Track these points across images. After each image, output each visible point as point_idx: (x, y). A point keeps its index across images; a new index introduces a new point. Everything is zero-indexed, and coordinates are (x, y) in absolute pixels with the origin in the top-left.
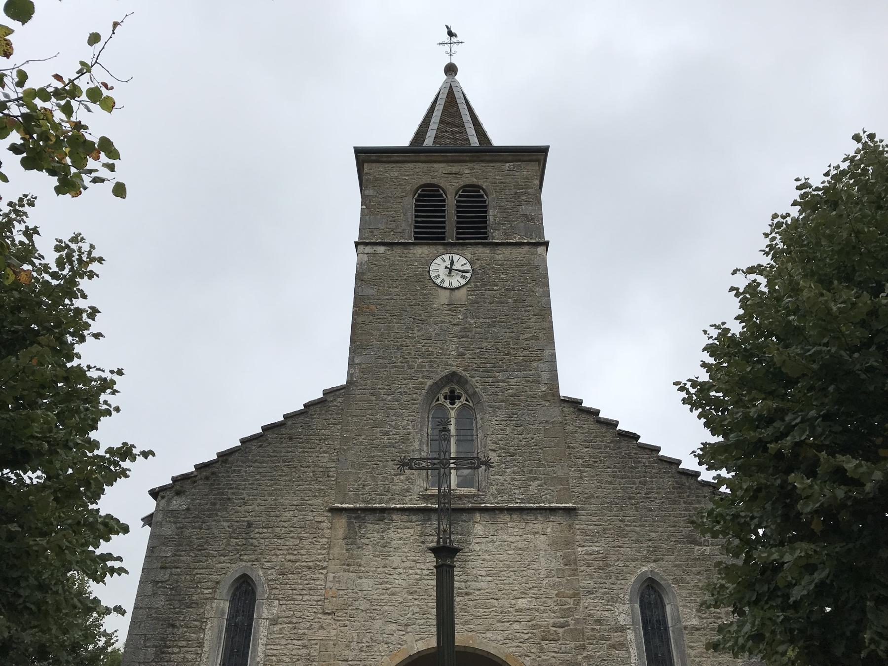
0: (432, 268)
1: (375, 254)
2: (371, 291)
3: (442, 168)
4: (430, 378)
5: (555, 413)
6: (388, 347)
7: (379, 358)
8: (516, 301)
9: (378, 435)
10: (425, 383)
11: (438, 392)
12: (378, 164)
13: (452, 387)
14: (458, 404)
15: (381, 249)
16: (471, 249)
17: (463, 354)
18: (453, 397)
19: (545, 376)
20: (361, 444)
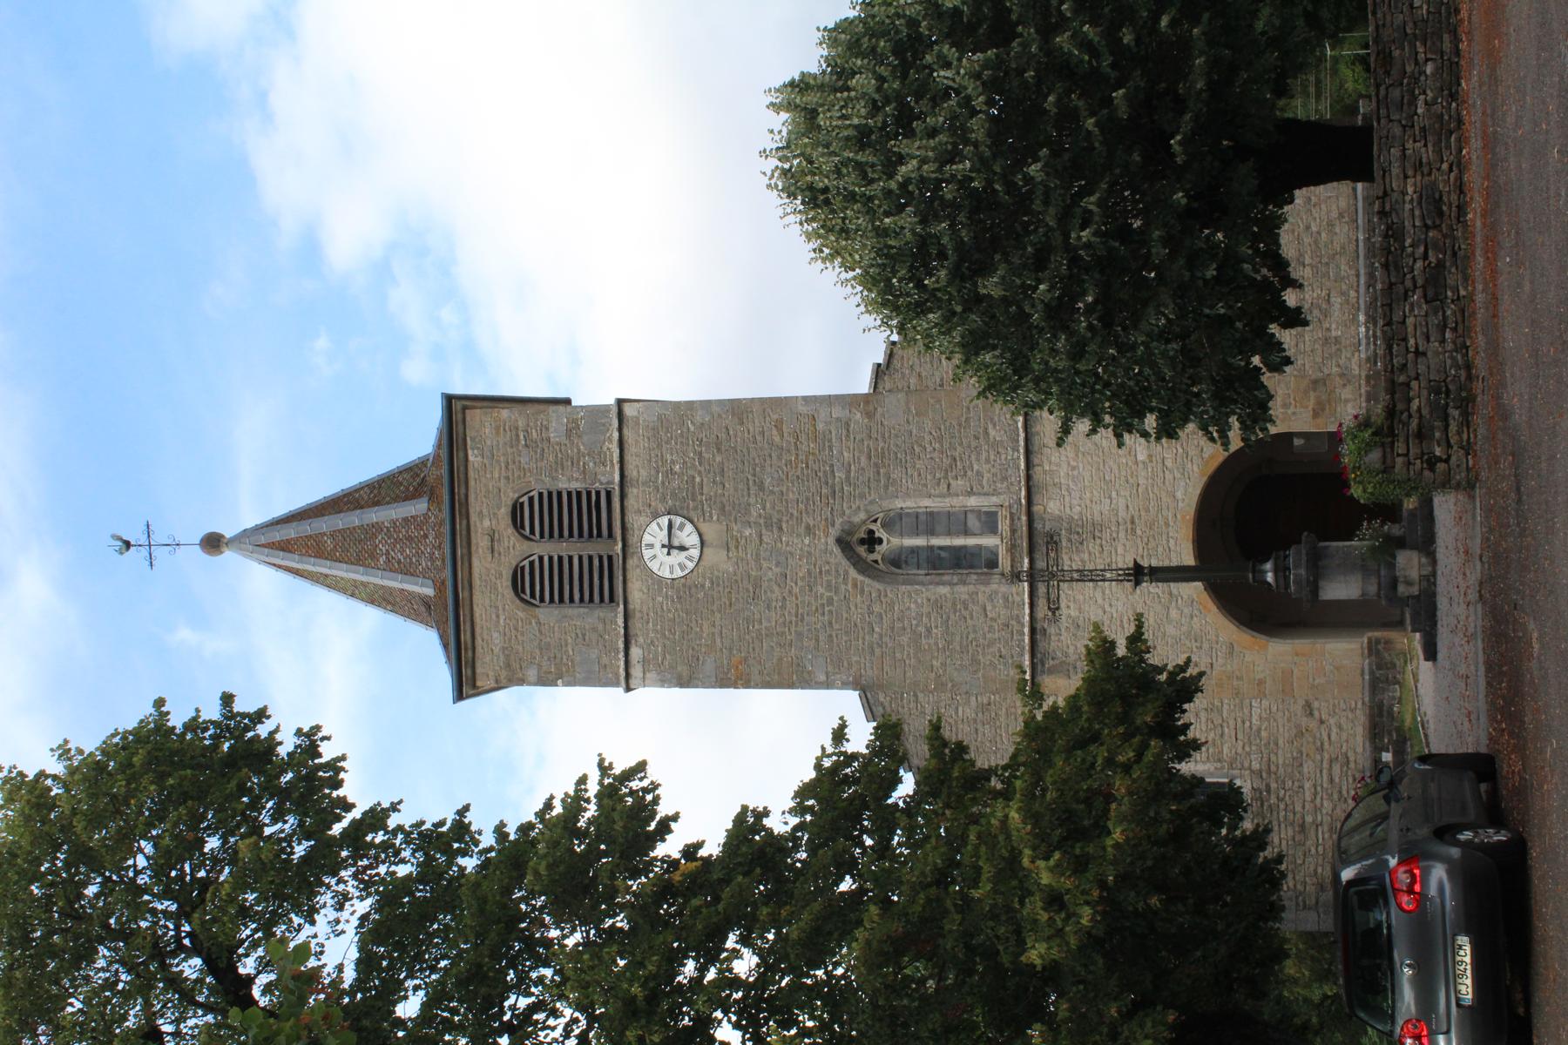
0: (667, 575)
1: (645, 662)
2: (709, 666)
3: (481, 564)
4: (846, 573)
5: (893, 404)
6: (799, 635)
7: (817, 648)
8: (719, 450)
9: (932, 641)
10: (854, 580)
11: (865, 561)
12: (478, 665)
13: (859, 546)
14: (880, 533)
15: (636, 652)
16: (630, 518)
17: (808, 528)
18: (871, 541)
19: (837, 412)
20: (944, 665)
